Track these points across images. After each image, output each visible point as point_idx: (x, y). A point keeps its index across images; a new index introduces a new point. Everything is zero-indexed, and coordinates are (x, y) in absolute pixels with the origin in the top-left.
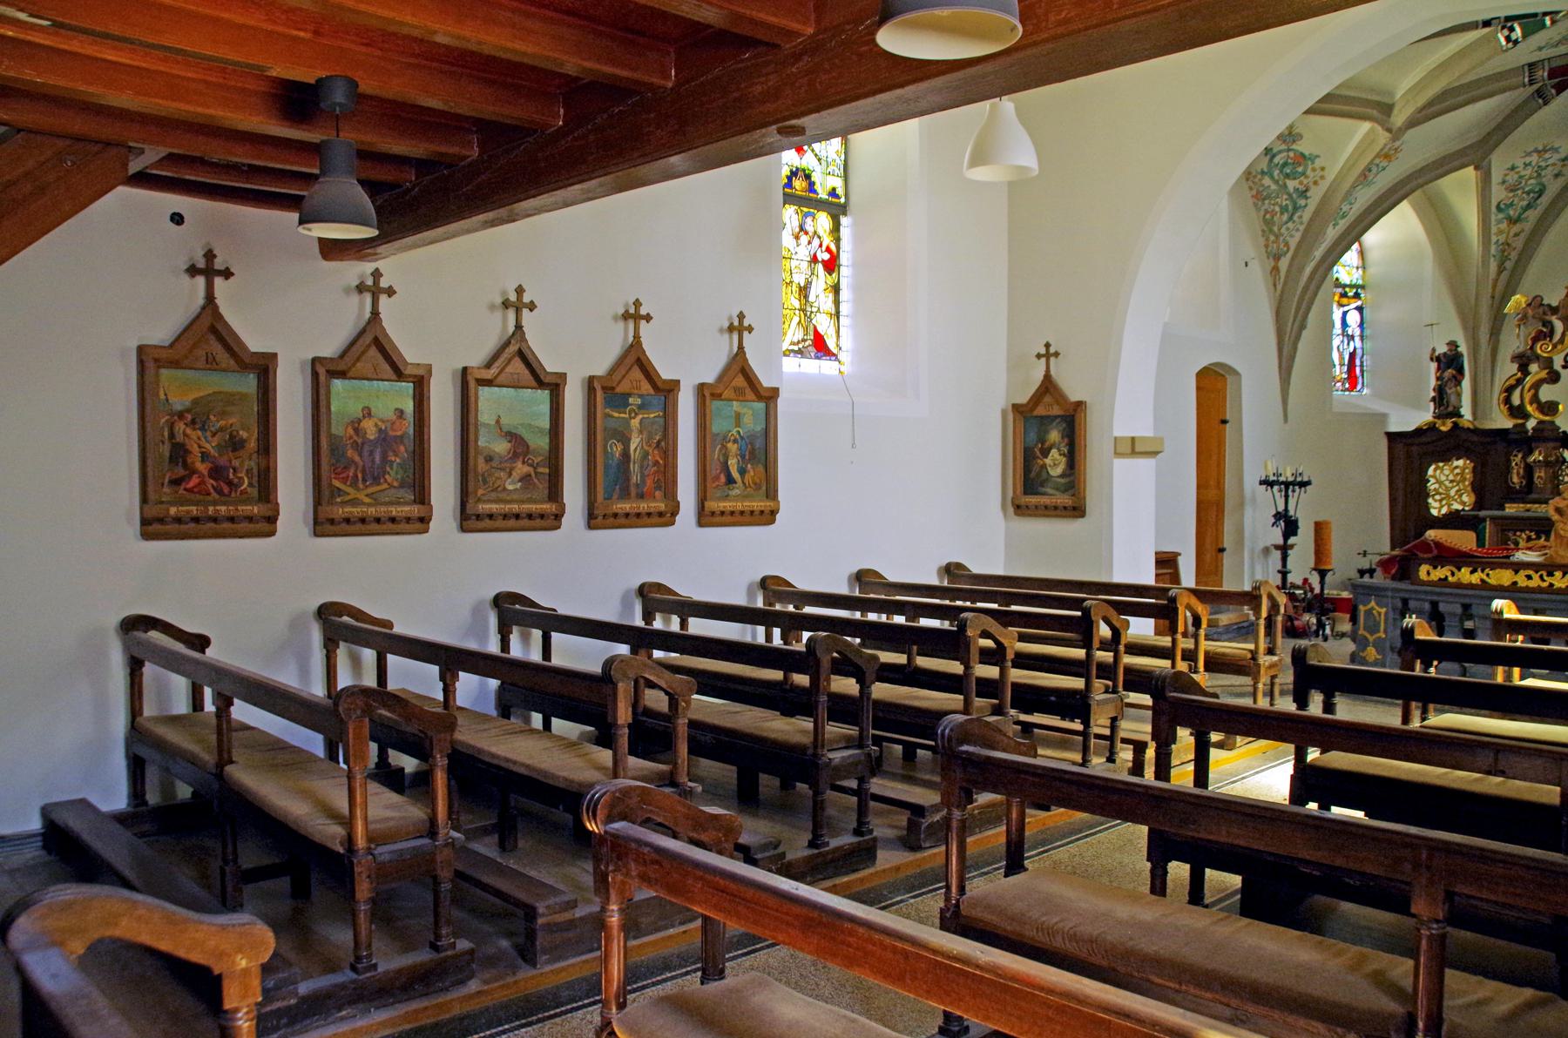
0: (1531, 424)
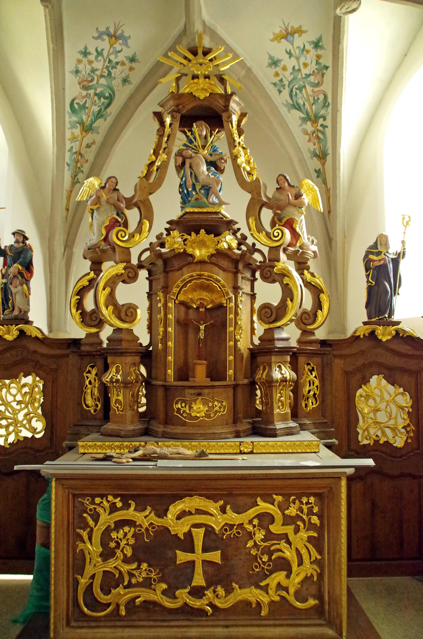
0: (106, 333)
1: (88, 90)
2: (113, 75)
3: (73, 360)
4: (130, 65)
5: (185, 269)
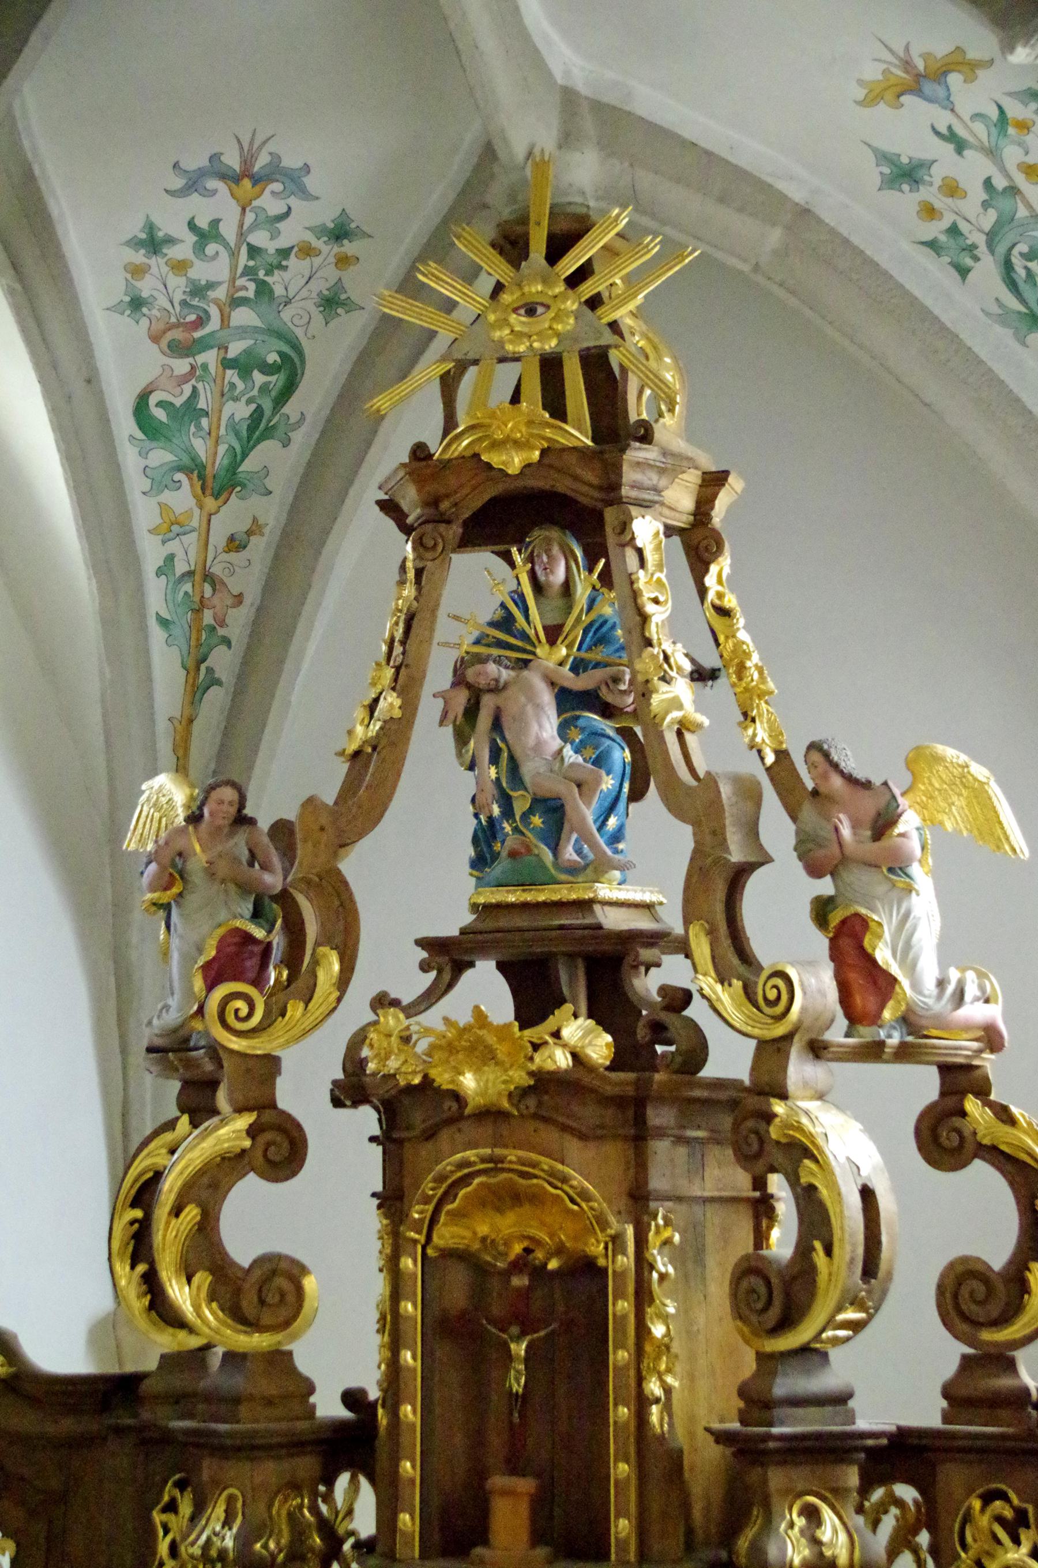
1: (193, 356)
2: (279, 291)
3: (118, 1459)
4: (336, 249)
5: (445, 1135)
